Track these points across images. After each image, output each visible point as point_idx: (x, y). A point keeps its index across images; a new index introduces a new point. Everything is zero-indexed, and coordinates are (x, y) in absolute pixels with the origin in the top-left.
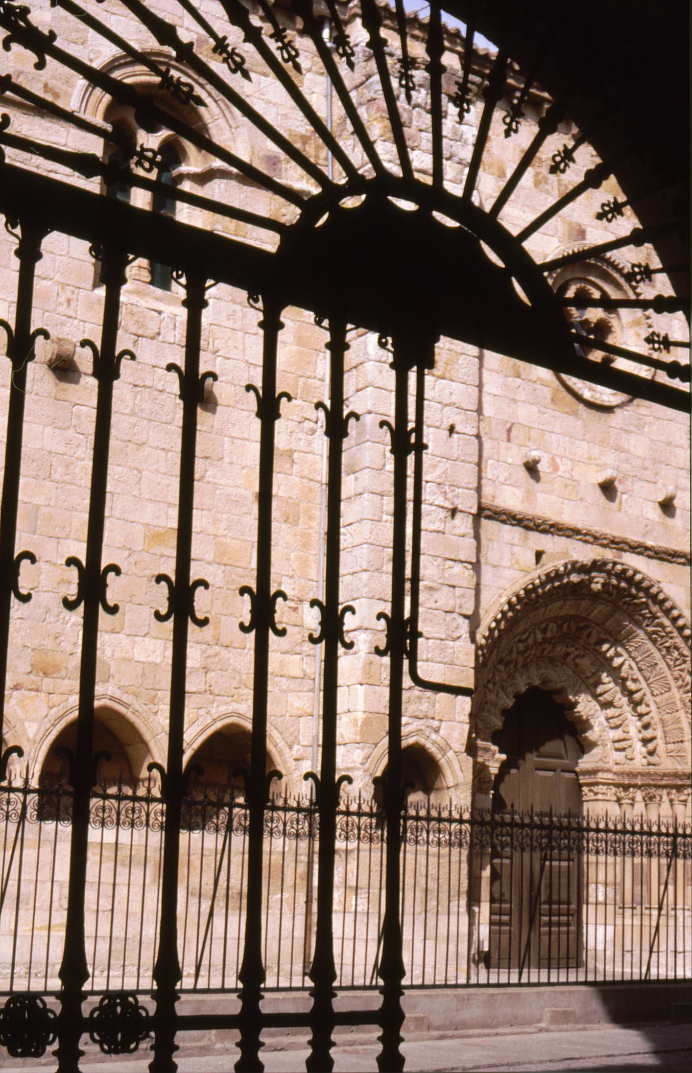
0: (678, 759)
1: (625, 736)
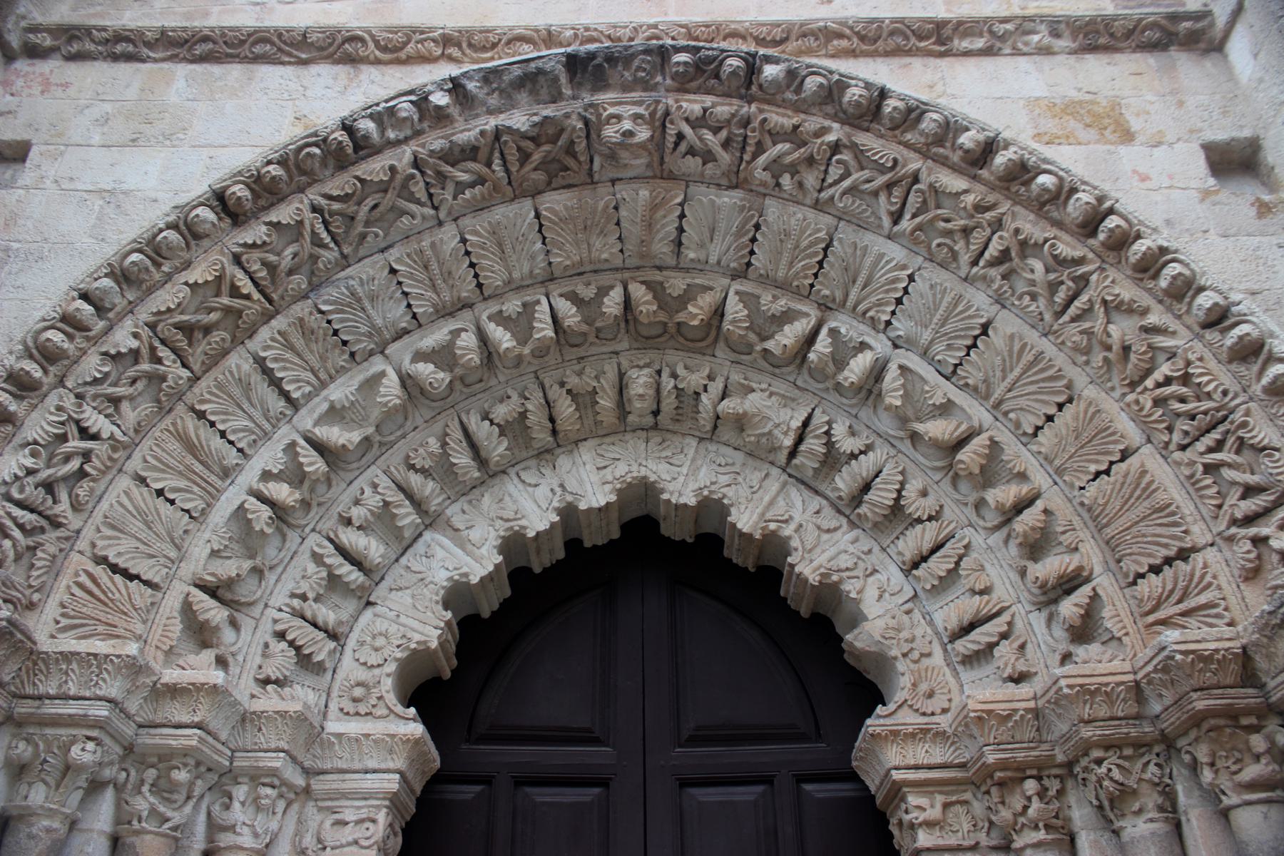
0: (1192, 622)
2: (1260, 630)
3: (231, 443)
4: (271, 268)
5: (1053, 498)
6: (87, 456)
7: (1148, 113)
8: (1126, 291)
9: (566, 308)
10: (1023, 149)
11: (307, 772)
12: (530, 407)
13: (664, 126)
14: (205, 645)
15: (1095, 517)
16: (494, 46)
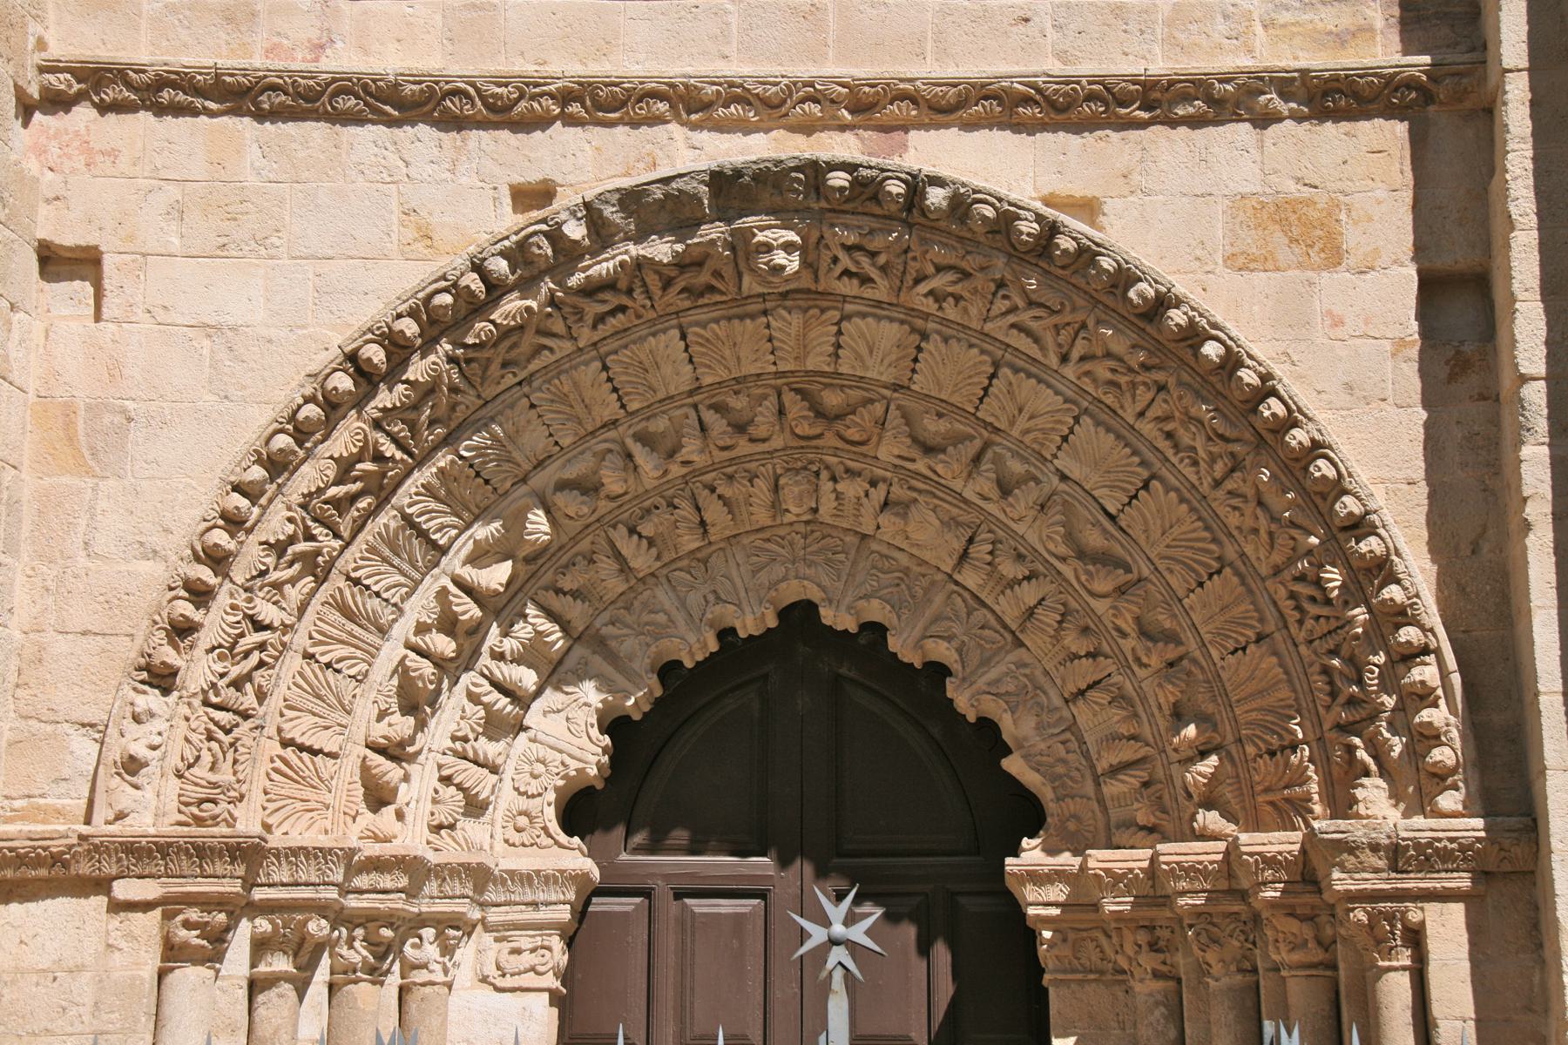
3: (386, 600)
4: (413, 427)
10: (1193, 309)
16: (624, 104)
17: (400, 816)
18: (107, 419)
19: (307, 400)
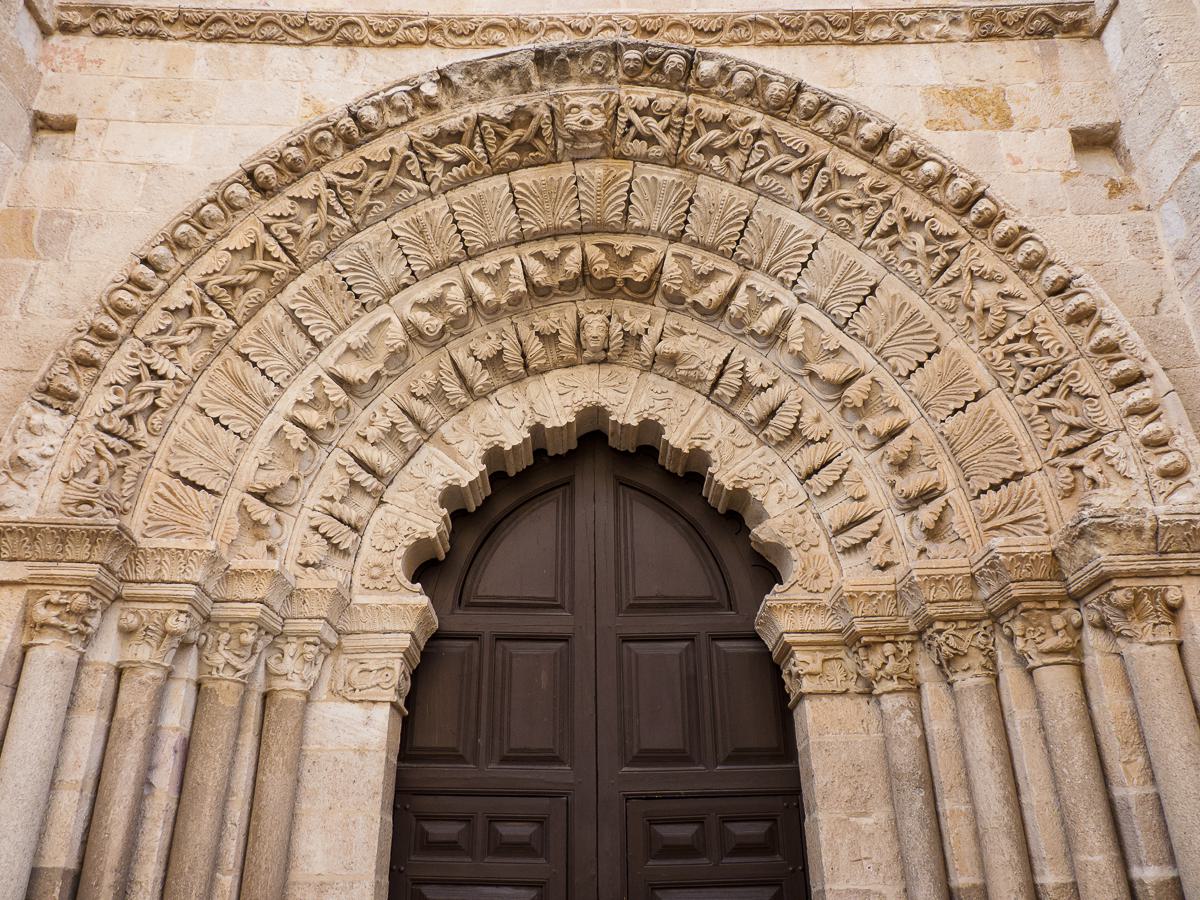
0: (1019, 529)
1: (851, 510)
2: (1065, 539)
5: (919, 427)
6: (157, 391)
7: (1028, 99)
8: (990, 262)
9: (534, 265)
11: (339, 633)
12: (506, 345)
13: (616, 115)
14: (258, 538)
15: (951, 444)
16: (472, 32)
17: (270, 550)
18: (56, 222)
19: (213, 201)
